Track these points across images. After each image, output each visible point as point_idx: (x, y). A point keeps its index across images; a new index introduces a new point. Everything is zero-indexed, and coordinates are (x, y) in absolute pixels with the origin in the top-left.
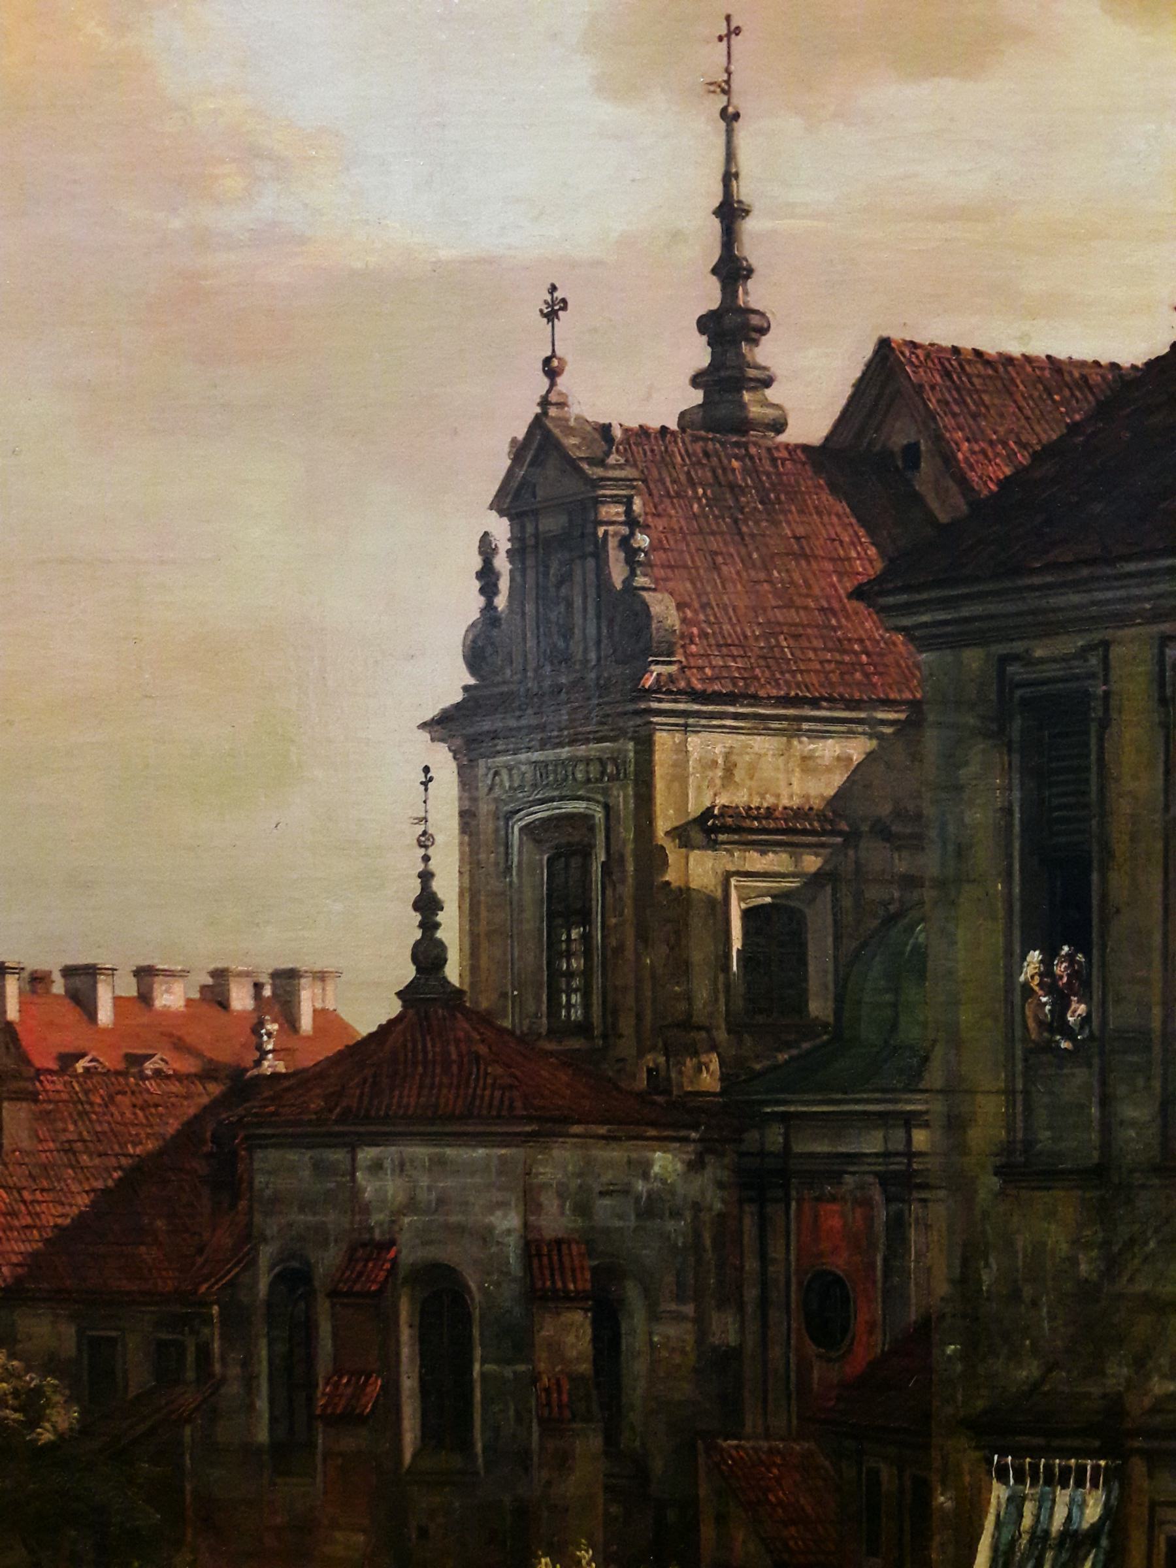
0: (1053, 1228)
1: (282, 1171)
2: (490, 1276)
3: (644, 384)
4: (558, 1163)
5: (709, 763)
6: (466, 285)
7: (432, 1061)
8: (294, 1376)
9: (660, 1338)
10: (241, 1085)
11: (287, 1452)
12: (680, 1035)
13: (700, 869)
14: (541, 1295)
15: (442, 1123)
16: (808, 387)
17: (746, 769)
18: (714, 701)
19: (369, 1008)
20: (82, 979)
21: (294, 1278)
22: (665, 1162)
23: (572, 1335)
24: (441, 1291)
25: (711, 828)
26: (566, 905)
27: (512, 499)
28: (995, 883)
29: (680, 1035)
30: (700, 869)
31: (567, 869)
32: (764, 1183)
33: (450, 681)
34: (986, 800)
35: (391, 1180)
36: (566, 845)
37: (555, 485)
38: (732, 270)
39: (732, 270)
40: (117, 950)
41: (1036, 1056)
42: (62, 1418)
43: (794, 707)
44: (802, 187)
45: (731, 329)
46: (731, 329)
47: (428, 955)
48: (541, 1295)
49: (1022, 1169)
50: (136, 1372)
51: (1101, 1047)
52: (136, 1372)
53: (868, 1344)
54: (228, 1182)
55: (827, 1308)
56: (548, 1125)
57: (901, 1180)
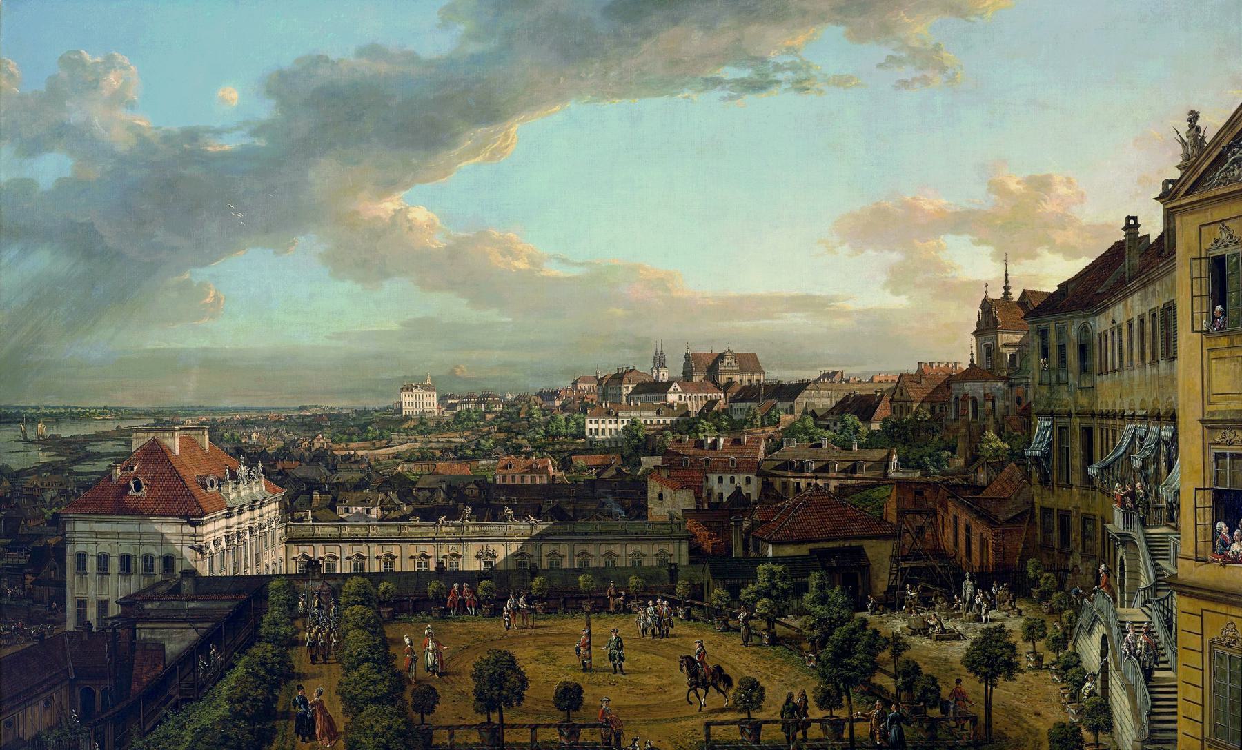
0: (1045, 390)
1: (954, 386)
2: (980, 399)
3: (997, 294)
4: (988, 384)
5: (1004, 338)
6: (976, 283)
7: (972, 373)
8: (957, 411)
9: (1000, 404)
10: (951, 376)
11: (955, 420)
12: (1002, 369)
13: (1004, 350)
14: (986, 400)
15: (974, 380)
16: (1016, 295)
17: (1008, 339)
18: (1006, 330)
19: (965, 367)
20: (931, 364)
21: (957, 399)
22: (1000, 384)
23: (990, 404)
24: (974, 400)
25: (1005, 345)
26: (988, 355)
27: (982, 307)
28: (1038, 350)
29: (1002, 369)
30: (1004, 350)
31: (988, 351)
32: (1011, 386)
33: (975, 328)
34: (1036, 341)
35: (968, 387)
36: (988, 348)
37: (987, 305)
38: (1007, 281)
39: (1007, 281)
40: (935, 360)
41: (1043, 370)
42: (929, 416)
43: (1015, 331)
44: (1015, 271)
45: (1007, 288)
46: (1007, 288)
47: (972, 361)
48: (986, 400)
49: (1041, 384)
50: (938, 410)
51: (1049, 369)
52: (938, 410)
53: (1024, 404)
54: (949, 387)
55: (1019, 401)
56: (987, 380)
57: (1027, 386)
